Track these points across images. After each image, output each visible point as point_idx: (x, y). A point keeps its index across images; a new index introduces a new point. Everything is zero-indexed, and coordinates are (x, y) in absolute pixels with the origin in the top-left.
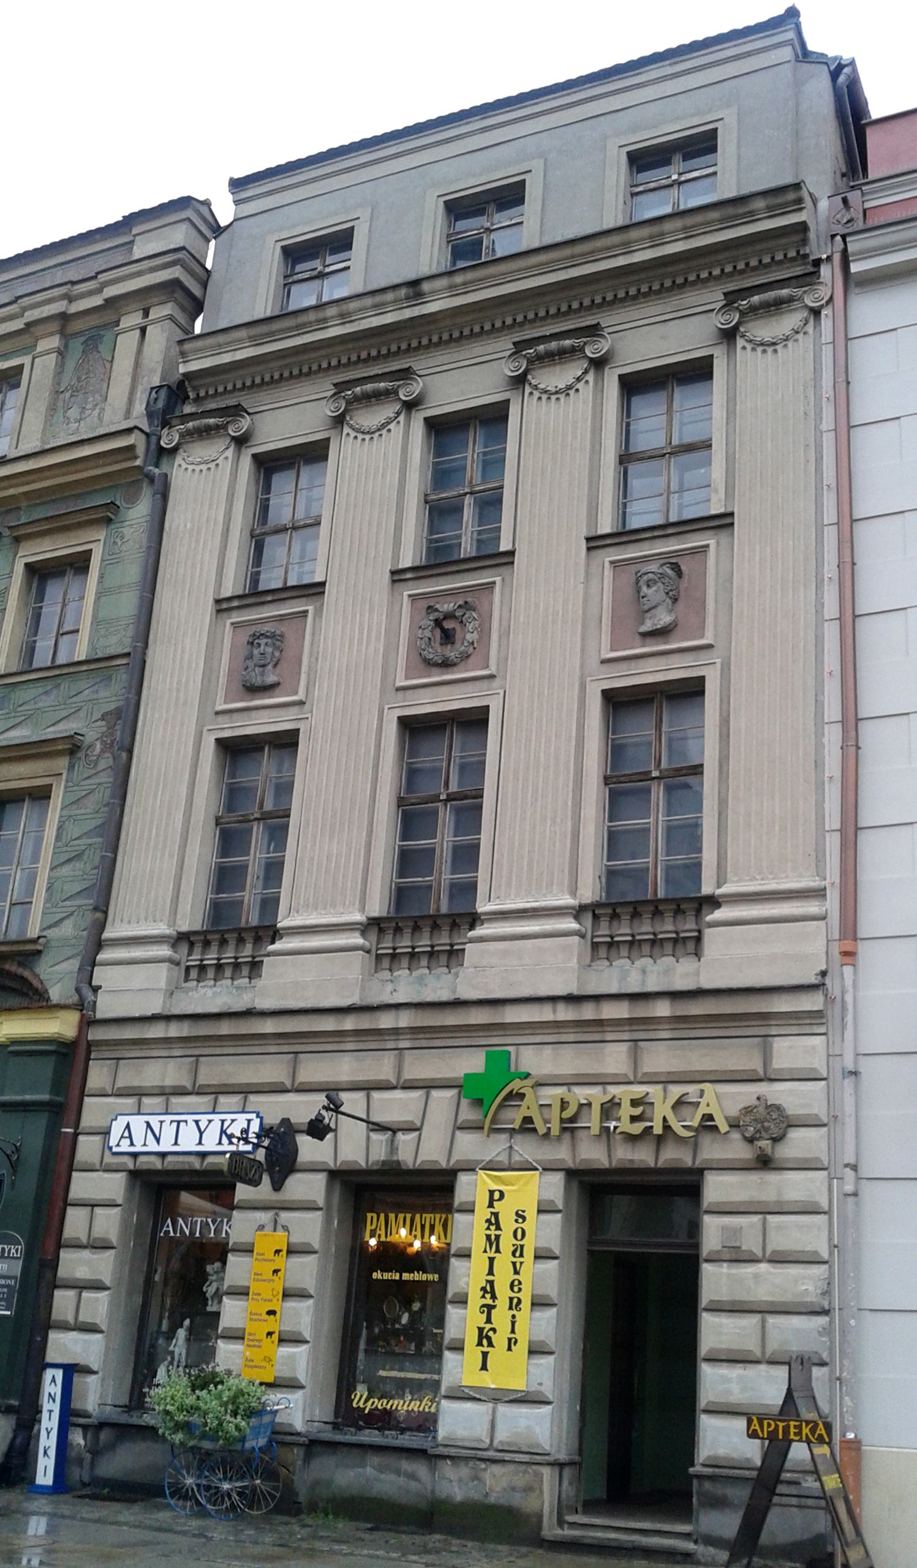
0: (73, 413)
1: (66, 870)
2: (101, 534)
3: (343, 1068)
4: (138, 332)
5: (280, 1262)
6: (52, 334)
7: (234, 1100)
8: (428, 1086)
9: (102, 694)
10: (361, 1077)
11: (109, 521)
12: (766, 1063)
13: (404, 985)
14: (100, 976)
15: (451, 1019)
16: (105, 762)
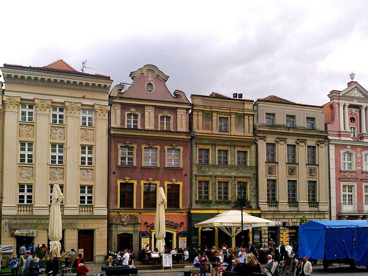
0: (238, 128)
1: (251, 193)
2: (249, 149)
3: (289, 217)
4: (248, 120)
5: (286, 235)
6: (234, 115)
7: (278, 220)
8: (297, 219)
9: (252, 171)
10: (291, 218)
11: (249, 148)
12: (324, 217)
13: (292, 209)
14: (260, 206)
15: (300, 213)
16: (254, 180)
